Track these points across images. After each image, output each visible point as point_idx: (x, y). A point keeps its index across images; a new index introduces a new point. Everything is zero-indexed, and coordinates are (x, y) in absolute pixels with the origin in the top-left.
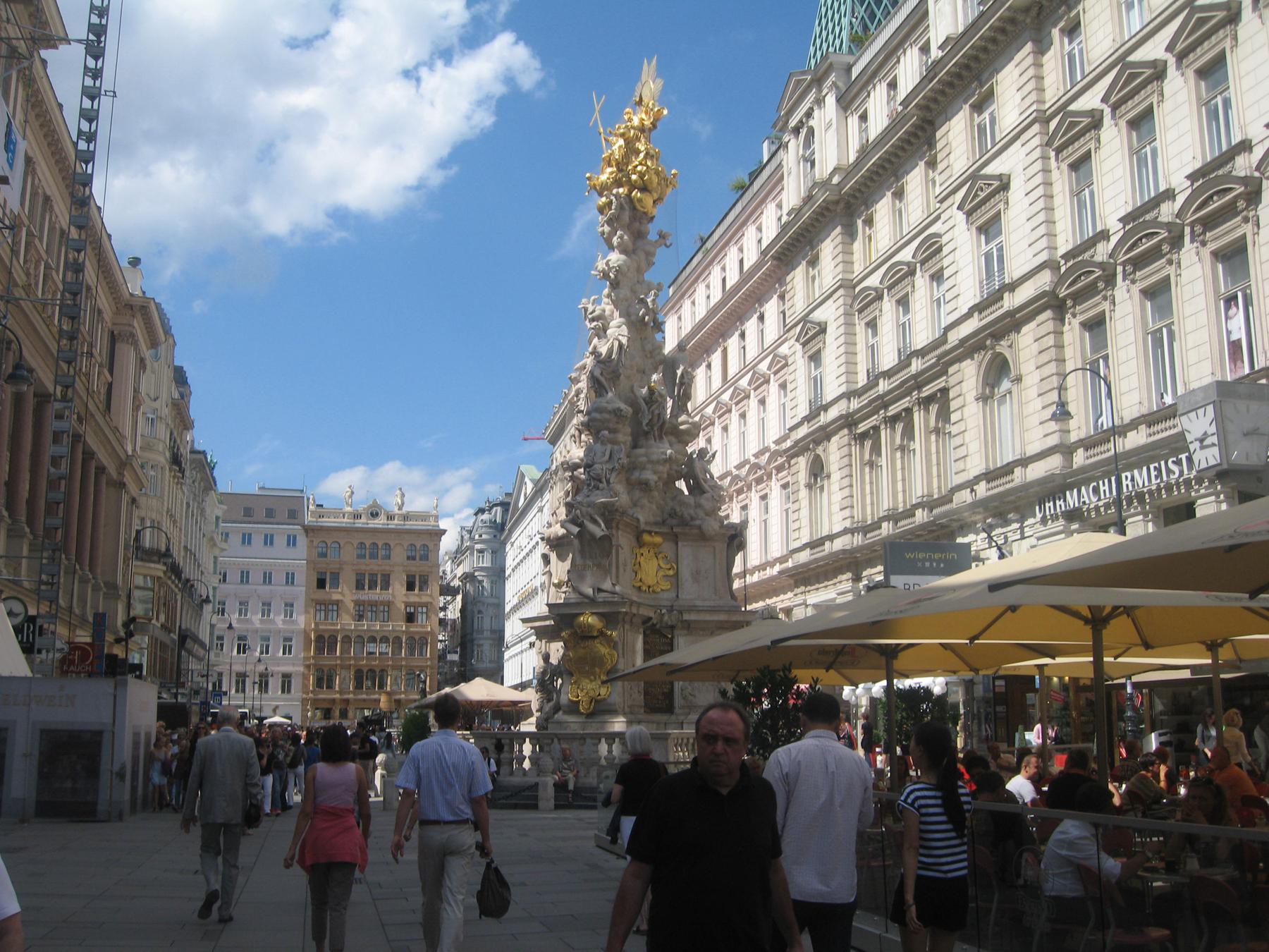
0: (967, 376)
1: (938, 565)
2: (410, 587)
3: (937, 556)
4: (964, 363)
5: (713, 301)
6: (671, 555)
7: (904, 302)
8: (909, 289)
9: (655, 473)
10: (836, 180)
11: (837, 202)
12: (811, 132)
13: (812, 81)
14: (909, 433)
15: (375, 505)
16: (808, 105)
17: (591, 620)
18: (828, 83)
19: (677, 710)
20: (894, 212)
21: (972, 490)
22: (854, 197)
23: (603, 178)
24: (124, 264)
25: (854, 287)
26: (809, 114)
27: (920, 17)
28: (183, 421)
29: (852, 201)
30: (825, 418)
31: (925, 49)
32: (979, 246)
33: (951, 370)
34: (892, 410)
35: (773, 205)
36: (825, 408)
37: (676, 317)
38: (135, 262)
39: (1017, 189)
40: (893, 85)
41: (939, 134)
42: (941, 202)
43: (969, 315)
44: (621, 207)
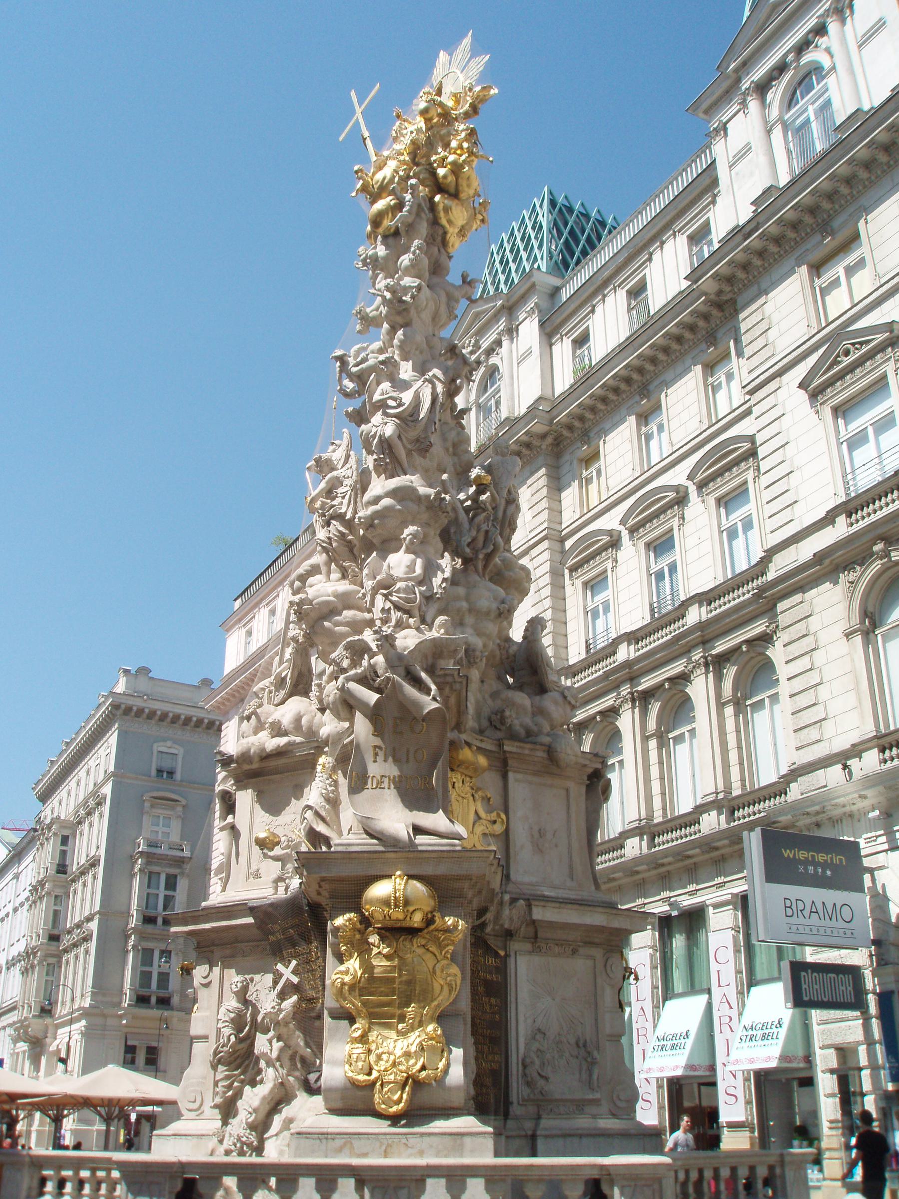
1: (824, 871)
3: (821, 857)
4: (813, 592)
6: (496, 799)
8: (675, 522)
9: (479, 634)
11: (544, 436)
12: (493, 371)
13: (503, 306)
14: (678, 708)
16: (494, 337)
18: (531, 304)
19: (516, 1109)
20: (639, 436)
21: (845, 767)
22: (570, 427)
23: (387, 172)
25: (562, 540)
27: (707, 186)
29: (566, 433)
31: (699, 236)
32: (837, 431)
33: (780, 607)
35: (267, 610)
37: (244, 631)
40: (638, 292)
41: (741, 316)
42: (751, 392)
43: (829, 519)
44: (417, 210)
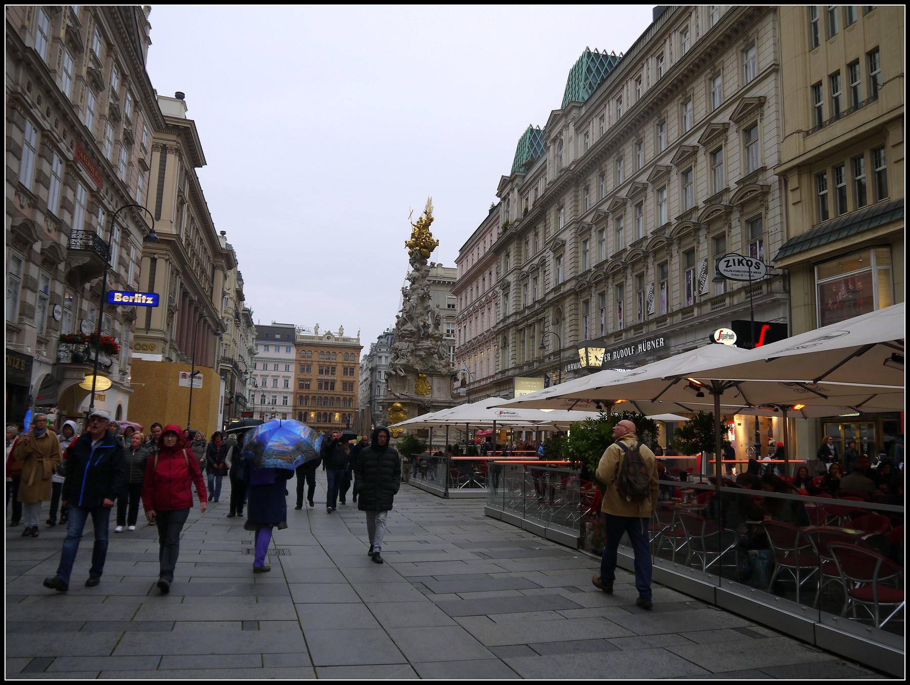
0: (550, 315)
2: (345, 373)
5: (475, 262)
7: (535, 279)
10: (516, 224)
15: (329, 333)
17: (399, 405)
24: (219, 234)
26: (508, 194)
27: (544, 168)
28: (240, 297)
30: (507, 322)
34: (530, 322)
36: (508, 317)
38: (223, 233)
39: (568, 247)
